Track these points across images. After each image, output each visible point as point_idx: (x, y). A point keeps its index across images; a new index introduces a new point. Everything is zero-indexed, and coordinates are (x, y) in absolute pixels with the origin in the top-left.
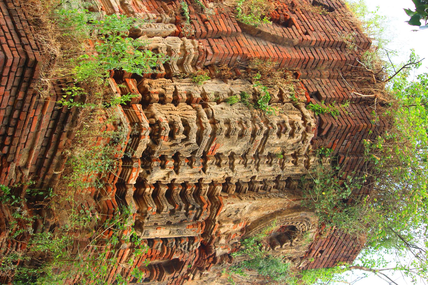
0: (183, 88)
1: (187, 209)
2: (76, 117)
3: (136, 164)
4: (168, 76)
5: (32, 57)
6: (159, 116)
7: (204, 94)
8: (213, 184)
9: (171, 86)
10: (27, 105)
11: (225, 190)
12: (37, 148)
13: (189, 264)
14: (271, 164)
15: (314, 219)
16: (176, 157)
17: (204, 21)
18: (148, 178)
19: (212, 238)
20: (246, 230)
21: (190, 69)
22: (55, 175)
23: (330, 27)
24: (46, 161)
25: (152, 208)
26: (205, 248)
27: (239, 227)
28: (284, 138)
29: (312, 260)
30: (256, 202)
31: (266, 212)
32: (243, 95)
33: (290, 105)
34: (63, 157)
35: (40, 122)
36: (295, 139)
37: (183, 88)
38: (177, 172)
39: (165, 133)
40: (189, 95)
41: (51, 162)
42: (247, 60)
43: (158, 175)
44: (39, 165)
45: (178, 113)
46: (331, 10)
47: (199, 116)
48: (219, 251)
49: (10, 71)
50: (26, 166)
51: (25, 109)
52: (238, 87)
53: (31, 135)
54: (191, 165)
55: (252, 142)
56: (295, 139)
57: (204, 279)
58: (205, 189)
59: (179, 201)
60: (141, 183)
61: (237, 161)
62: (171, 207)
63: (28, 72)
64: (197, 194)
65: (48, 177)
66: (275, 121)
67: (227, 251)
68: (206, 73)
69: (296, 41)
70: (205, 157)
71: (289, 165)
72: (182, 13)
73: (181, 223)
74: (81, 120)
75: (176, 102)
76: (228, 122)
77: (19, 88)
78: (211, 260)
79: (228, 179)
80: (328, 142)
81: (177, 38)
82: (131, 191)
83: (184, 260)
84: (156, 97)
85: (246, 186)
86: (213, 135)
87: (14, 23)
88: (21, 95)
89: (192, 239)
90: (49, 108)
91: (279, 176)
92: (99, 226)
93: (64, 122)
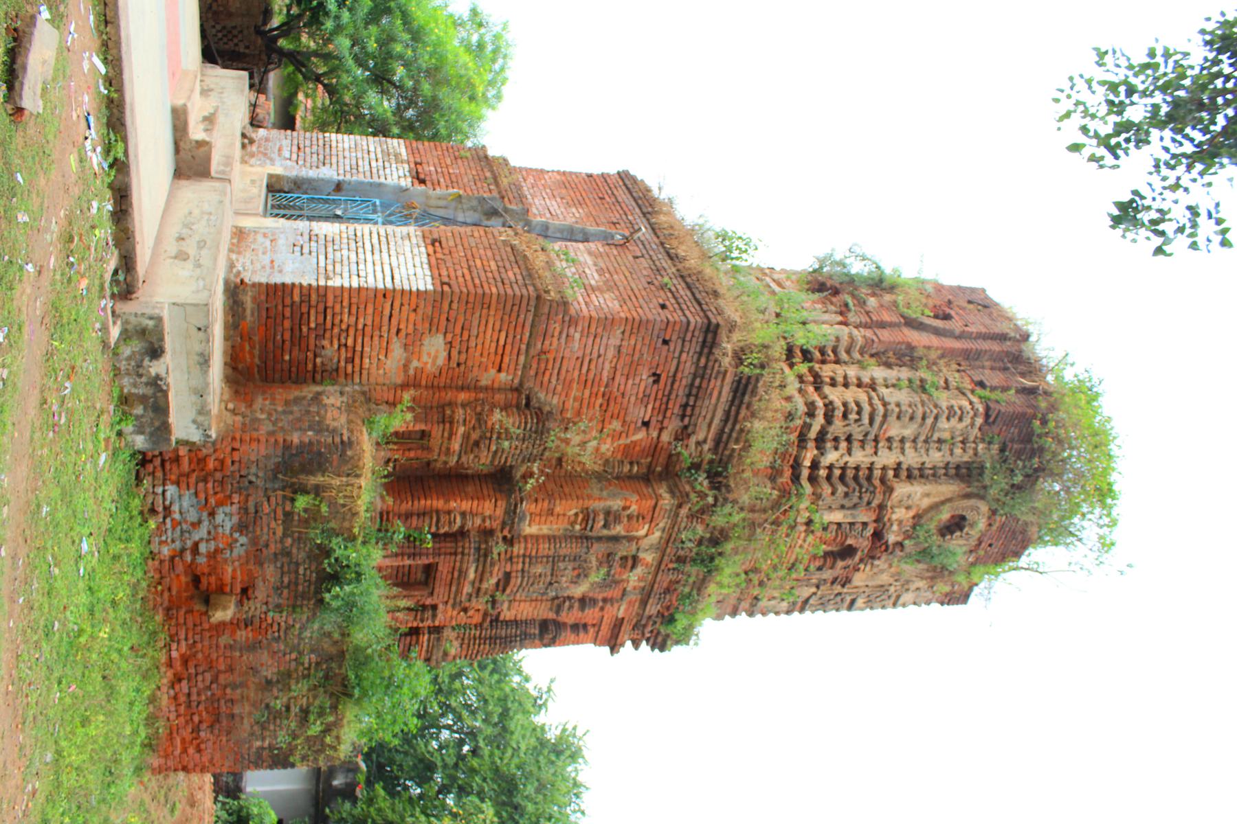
0: (852, 372)
1: (860, 492)
2: (756, 387)
3: (811, 445)
4: (837, 362)
5: (714, 321)
6: (831, 397)
7: (873, 379)
8: (884, 468)
9: (840, 370)
10: (709, 372)
11: (896, 476)
12: (716, 421)
14: (940, 450)
15: (984, 508)
16: (849, 439)
17: (868, 313)
18: (822, 459)
20: (918, 517)
21: (857, 356)
22: (733, 450)
23: (988, 322)
24: (725, 436)
25: (827, 489)
26: (878, 535)
27: (911, 513)
28: (954, 421)
29: (981, 553)
30: (928, 488)
31: (937, 499)
32: (910, 381)
33: (956, 392)
34: (742, 430)
35: (720, 393)
36: (964, 424)
37: (852, 372)
38: (850, 454)
39: (839, 413)
40: (859, 379)
41: (730, 436)
42: (911, 348)
43: (831, 457)
44: (718, 442)
45: (852, 394)
46: (985, 307)
47: (870, 399)
50: (705, 441)
51: (707, 376)
52: (905, 373)
53: (711, 407)
54: (863, 448)
55: (922, 425)
56: (964, 424)
57: (875, 570)
58: (877, 473)
59: (852, 484)
60: (815, 465)
61: (908, 445)
62: (845, 489)
63: (710, 336)
64: (869, 478)
65: (727, 453)
66: (944, 405)
67: (899, 539)
68: (873, 361)
69: (957, 332)
70: (876, 440)
71: (958, 451)
72: (846, 305)
73: (855, 506)
74: (761, 391)
75: (846, 385)
76: (898, 405)
77: (700, 354)
78: (883, 548)
79: (899, 464)
80: (996, 429)
81: (843, 327)
82: (805, 473)
84: (827, 380)
85: (916, 473)
86: (885, 416)
87: (693, 294)
88: (703, 361)
89: (865, 524)
90: (729, 378)
91: (948, 463)
92: (776, 505)
93: (744, 394)
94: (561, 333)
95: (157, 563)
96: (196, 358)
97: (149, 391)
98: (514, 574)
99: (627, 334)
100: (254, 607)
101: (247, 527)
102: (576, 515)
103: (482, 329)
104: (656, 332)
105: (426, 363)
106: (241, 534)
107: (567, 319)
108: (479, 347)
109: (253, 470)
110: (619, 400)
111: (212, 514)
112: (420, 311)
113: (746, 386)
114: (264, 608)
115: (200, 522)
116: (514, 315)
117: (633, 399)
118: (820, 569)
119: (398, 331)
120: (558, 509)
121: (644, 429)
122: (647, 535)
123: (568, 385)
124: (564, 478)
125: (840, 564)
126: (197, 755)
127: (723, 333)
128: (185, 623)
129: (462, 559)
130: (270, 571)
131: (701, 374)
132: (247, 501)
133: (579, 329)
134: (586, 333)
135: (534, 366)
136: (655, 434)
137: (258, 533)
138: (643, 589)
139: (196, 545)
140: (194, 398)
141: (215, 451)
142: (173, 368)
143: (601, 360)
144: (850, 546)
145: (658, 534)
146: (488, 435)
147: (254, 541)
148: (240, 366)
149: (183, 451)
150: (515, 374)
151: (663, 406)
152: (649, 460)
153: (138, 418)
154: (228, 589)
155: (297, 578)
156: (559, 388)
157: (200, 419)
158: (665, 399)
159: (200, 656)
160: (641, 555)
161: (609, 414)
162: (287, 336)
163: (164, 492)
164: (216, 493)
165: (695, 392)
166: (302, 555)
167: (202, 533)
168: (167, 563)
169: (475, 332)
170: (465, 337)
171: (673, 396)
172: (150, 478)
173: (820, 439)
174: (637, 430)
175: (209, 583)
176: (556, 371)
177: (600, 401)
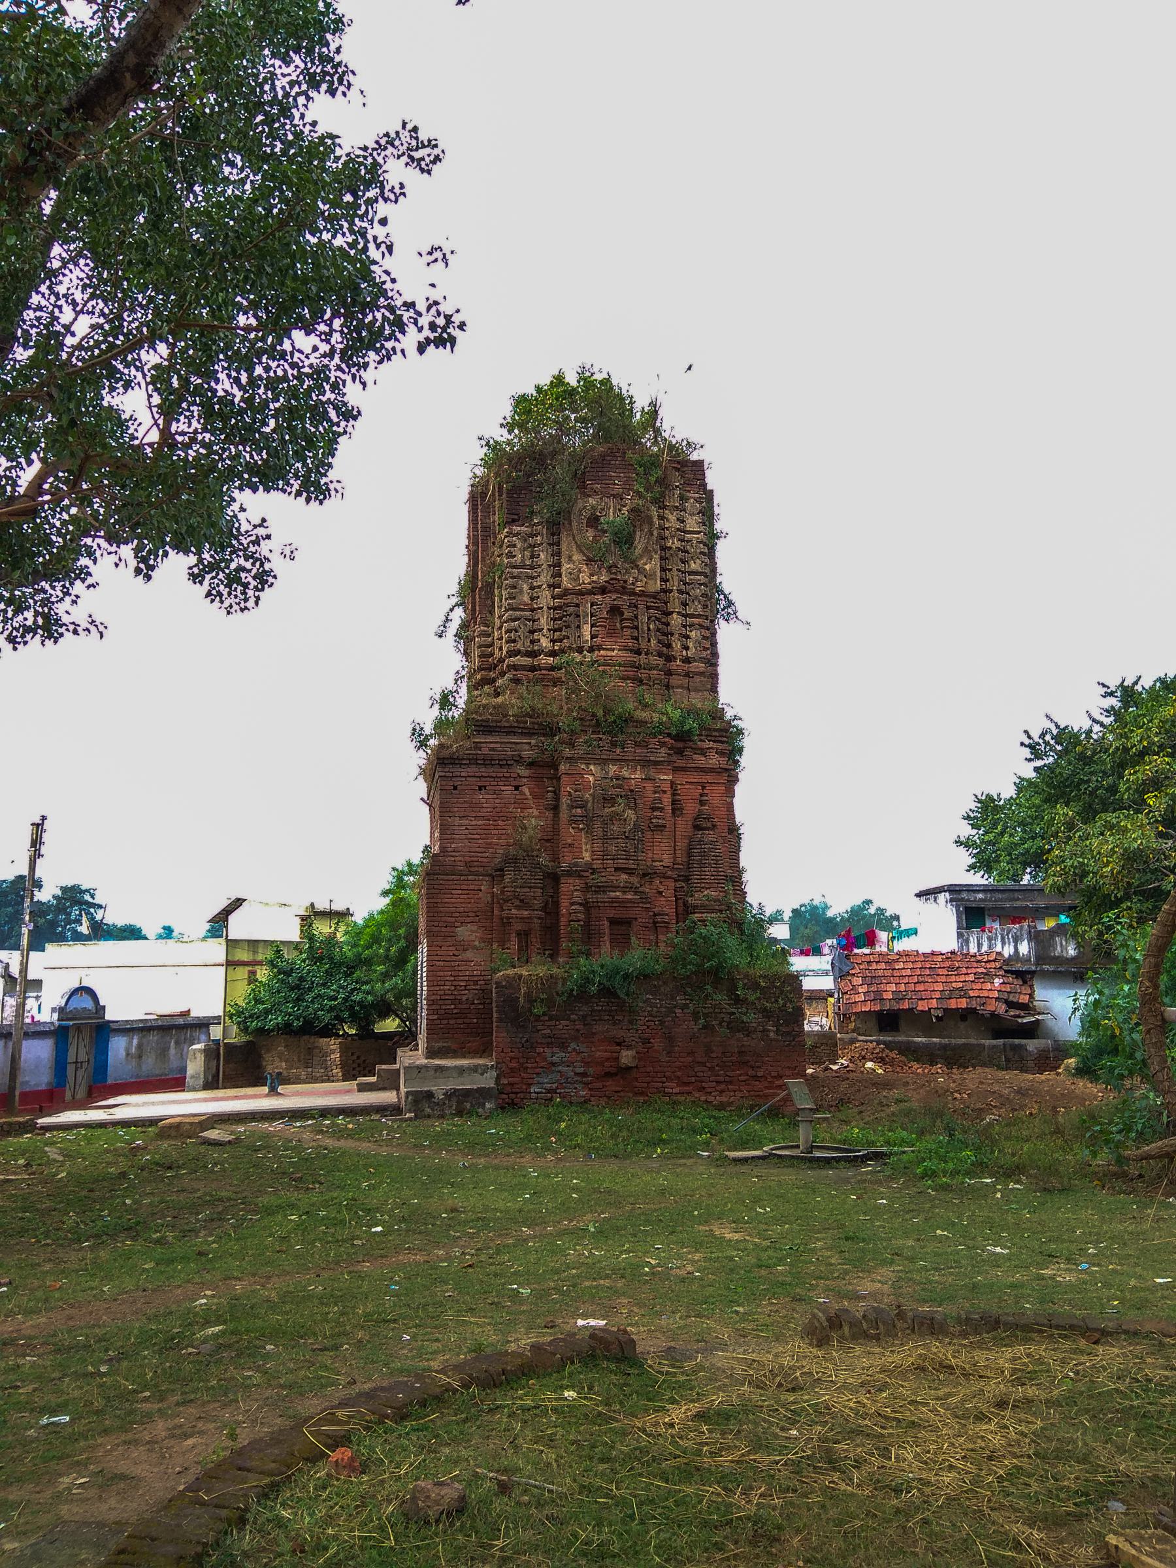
4: (492, 645)
8: (553, 598)
15: (580, 504)
16: (532, 632)
20: (589, 561)
26: (603, 591)
28: (516, 551)
43: (545, 643)
45: (505, 637)
48: (604, 578)
52: (496, 591)
60: (553, 654)
64: (560, 608)
67: (604, 571)
70: (532, 610)
97: (454, 1099)
111: (553, 1064)
118: (637, 628)
120: (569, 841)
124: (551, 839)
125: (627, 615)
127: (445, 753)
130: (598, 1028)
131: (474, 761)
134: (452, 840)
139: (576, 1074)
142: (439, 1088)
145: (592, 767)
147: (575, 1039)
148: (482, 1048)
153: (472, 1106)
159: (679, 1074)
161: (509, 815)
162: (460, 1021)
165: (488, 762)
167: (569, 1072)
173: (533, 654)
177: (500, 823)
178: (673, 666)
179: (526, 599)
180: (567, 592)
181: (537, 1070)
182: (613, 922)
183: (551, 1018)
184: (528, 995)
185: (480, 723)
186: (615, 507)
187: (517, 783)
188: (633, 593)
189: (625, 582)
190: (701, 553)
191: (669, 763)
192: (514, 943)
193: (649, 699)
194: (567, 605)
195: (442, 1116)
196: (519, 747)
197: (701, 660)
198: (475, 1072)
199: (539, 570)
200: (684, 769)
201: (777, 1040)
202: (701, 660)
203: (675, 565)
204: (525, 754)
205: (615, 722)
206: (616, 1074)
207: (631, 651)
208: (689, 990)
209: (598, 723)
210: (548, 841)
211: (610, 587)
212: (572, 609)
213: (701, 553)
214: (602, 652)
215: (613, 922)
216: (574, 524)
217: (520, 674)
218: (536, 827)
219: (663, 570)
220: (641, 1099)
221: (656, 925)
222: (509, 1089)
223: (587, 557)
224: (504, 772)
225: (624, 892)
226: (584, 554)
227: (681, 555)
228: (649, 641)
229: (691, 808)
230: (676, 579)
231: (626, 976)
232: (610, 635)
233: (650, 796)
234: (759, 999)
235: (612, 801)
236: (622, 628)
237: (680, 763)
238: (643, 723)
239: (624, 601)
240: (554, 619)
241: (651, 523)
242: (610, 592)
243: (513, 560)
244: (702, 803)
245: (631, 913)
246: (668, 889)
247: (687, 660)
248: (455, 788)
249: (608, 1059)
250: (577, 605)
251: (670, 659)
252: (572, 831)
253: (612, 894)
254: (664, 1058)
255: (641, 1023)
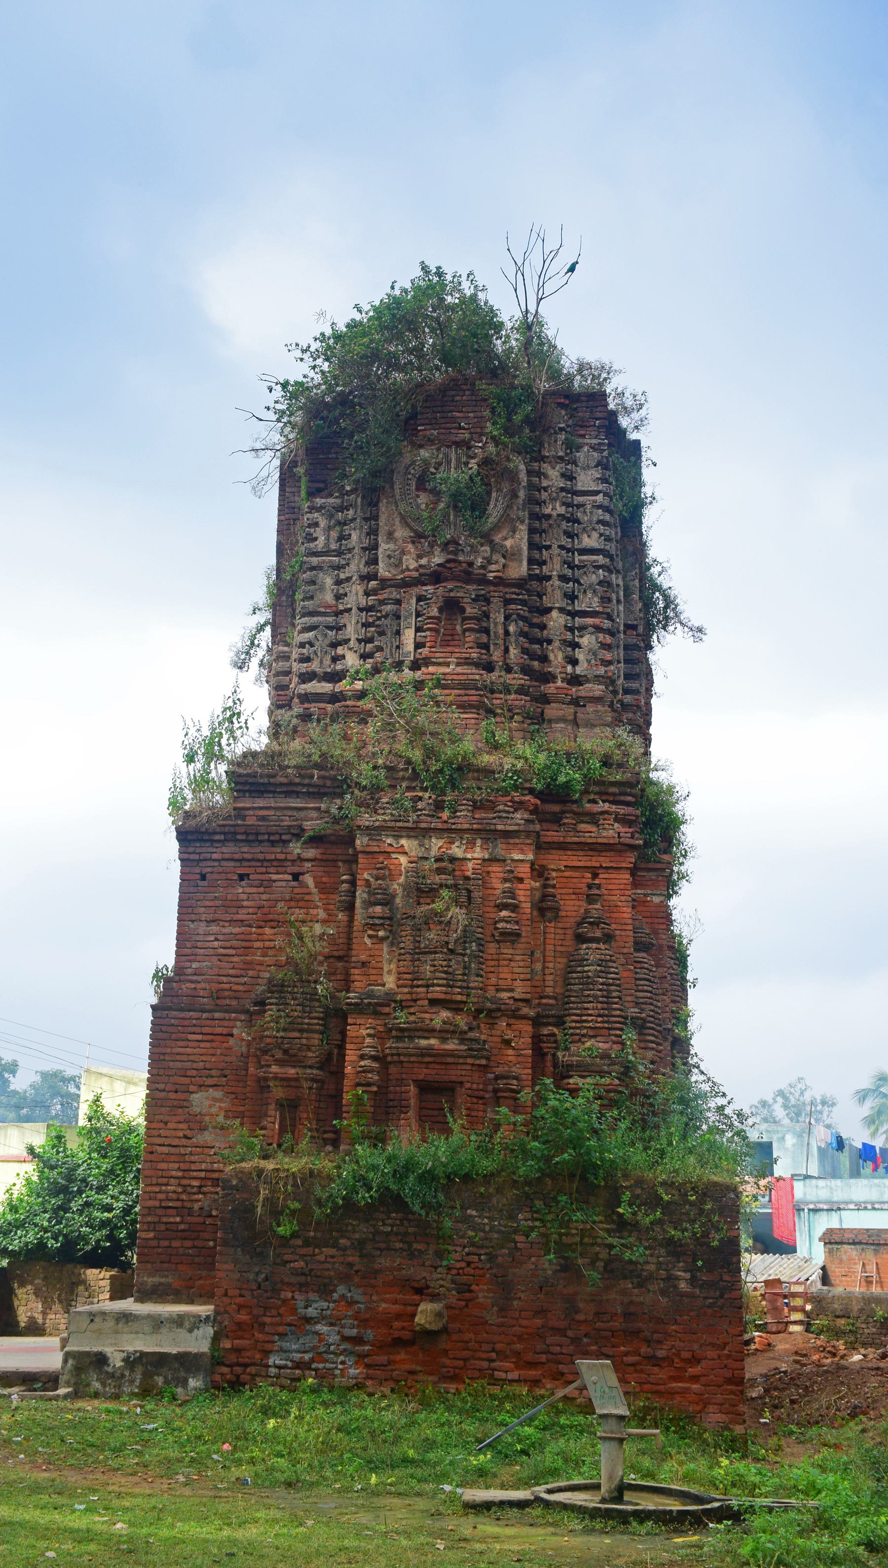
2: (248, 775)
3: (338, 687)
8: (367, 594)
10: (227, 829)
13: (451, 590)
14: (350, 535)
15: (407, 459)
16: (334, 645)
19: (420, 575)
26: (436, 578)
27: (410, 547)
31: (397, 521)
35: (261, 808)
41: (309, 785)
43: (351, 660)
49: (194, 853)
51: (232, 830)
61: (342, 576)
63: (189, 837)
65: (329, 783)
67: (437, 550)
70: (338, 613)
71: (351, 512)
77: (213, 841)
78: (452, 565)
83: (441, 599)
88: (217, 837)
89: (420, 599)
94: (192, 982)
95: (369, 1383)
96: (120, 1325)
98: (430, 996)
99: (193, 917)
100: (439, 1280)
101: (325, 1285)
102: (370, 936)
103: (185, 1058)
104: (192, 889)
105: (220, 1108)
106: (335, 1291)
107: (177, 978)
108: (204, 1058)
109: (251, 1276)
110: (266, 910)
111: (308, 1320)
112: (167, 1118)
113: (251, 784)
114: (439, 1270)
115: (317, 1333)
116: (170, 1029)
117: (264, 897)
118: (487, 631)
119: (185, 1137)
120: (363, 957)
121: (301, 878)
122: (406, 853)
123: (249, 965)
126: (703, 1364)
128: (465, 1360)
129: (405, 1055)
130: (383, 1262)
131: (230, 836)
132: (289, 1284)
133: (188, 964)
134: (193, 957)
135: (228, 1001)
136: (308, 865)
137: (332, 1273)
138: (486, 840)
139: (345, 1339)
140: (164, 1330)
141: (226, 1312)
143: (220, 937)
144: (441, 610)
145: (403, 842)
146: (280, 1041)
147: (345, 1278)
149: (227, 1344)
150: (235, 1020)
151: (275, 863)
152: (340, 864)
154: (409, 1309)
155: (397, 1234)
156: (251, 973)
157: (187, 1324)
158: (265, 864)
159: (518, 1347)
160: (434, 852)
163: (276, 1366)
164: (279, 1315)
165: (253, 837)
166: (363, 1228)
168: (370, 1372)
169: (202, 1064)
170: (194, 1073)
171: (261, 856)
172: (258, 1379)
173: (334, 677)
174: (304, 885)
175: (403, 1328)
176: (233, 979)
177: (267, 930)
178: (550, 689)
179: (329, 598)
180: (385, 583)
181: (281, 1329)
182: (425, 1088)
183: (307, 1243)
184: (270, 1202)
185: (252, 779)
186: (458, 460)
187: (296, 869)
188: (483, 581)
189: (471, 564)
190: (600, 522)
191: (528, 834)
192: (273, 1121)
193: (501, 737)
194: (382, 602)
195: (116, 1397)
196: (302, 814)
197: (597, 679)
198: (182, 1326)
199: (349, 556)
200: (562, 846)
201: (691, 1296)
202: (597, 679)
203: (556, 539)
204: (307, 825)
205: (441, 771)
206: (410, 1343)
207: (477, 665)
208: (539, 1204)
209: (415, 776)
210: (340, 958)
211: (446, 573)
212: (389, 608)
213: (600, 522)
214: (431, 669)
215: (425, 1088)
216: (397, 486)
217: (314, 708)
218: (321, 937)
219: (532, 546)
220: (452, 1387)
221: (501, 1093)
222: (233, 1358)
223: (415, 531)
224: (277, 852)
225: (444, 1040)
226: (411, 529)
227: (564, 525)
228: (506, 650)
229: (572, 907)
230: (557, 561)
231: (428, 1177)
232: (446, 643)
233: (499, 886)
234: (660, 1222)
235: (432, 893)
236: (464, 631)
237: (552, 835)
238: (488, 772)
239: (466, 593)
240: (366, 625)
241: (513, 476)
242: (446, 580)
243: (312, 545)
244: (591, 899)
245: (454, 1074)
246: (521, 1036)
247: (575, 680)
248: (203, 877)
249: (398, 1316)
250: (398, 602)
251: (549, 678)
252: (368, 941)
253: (423, 1042)
254: (492, 1318)
255: (457, 1256)
